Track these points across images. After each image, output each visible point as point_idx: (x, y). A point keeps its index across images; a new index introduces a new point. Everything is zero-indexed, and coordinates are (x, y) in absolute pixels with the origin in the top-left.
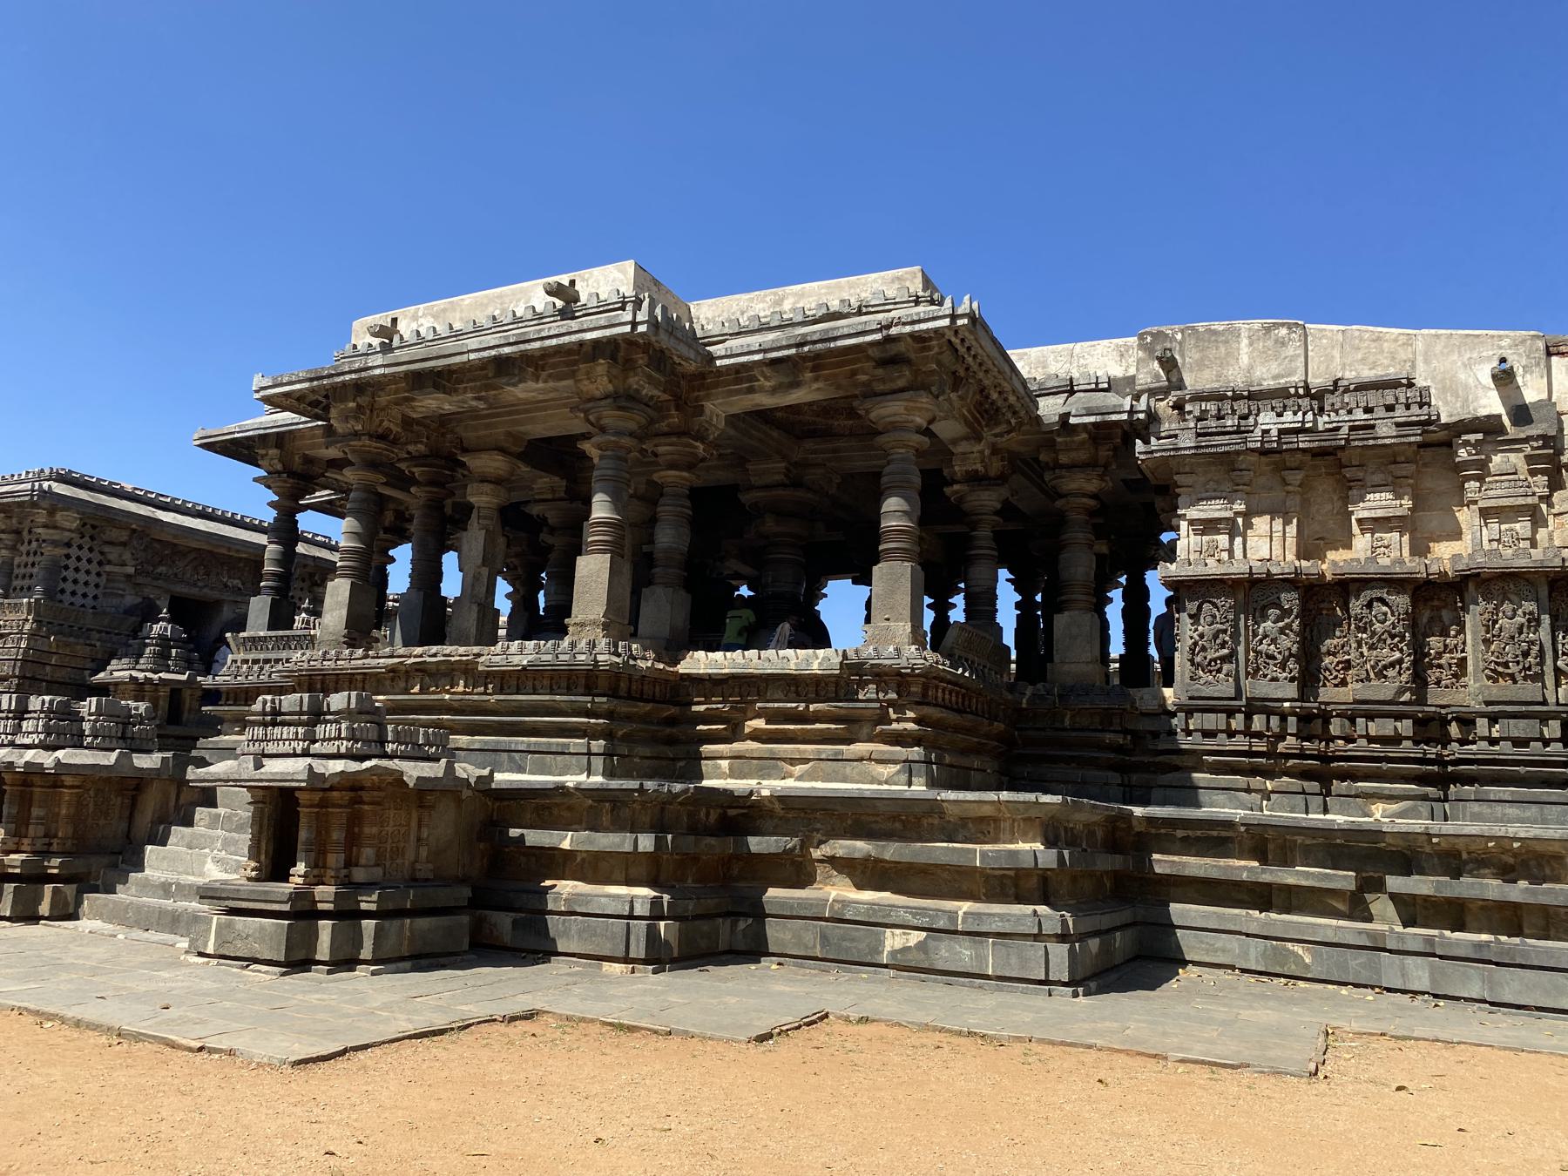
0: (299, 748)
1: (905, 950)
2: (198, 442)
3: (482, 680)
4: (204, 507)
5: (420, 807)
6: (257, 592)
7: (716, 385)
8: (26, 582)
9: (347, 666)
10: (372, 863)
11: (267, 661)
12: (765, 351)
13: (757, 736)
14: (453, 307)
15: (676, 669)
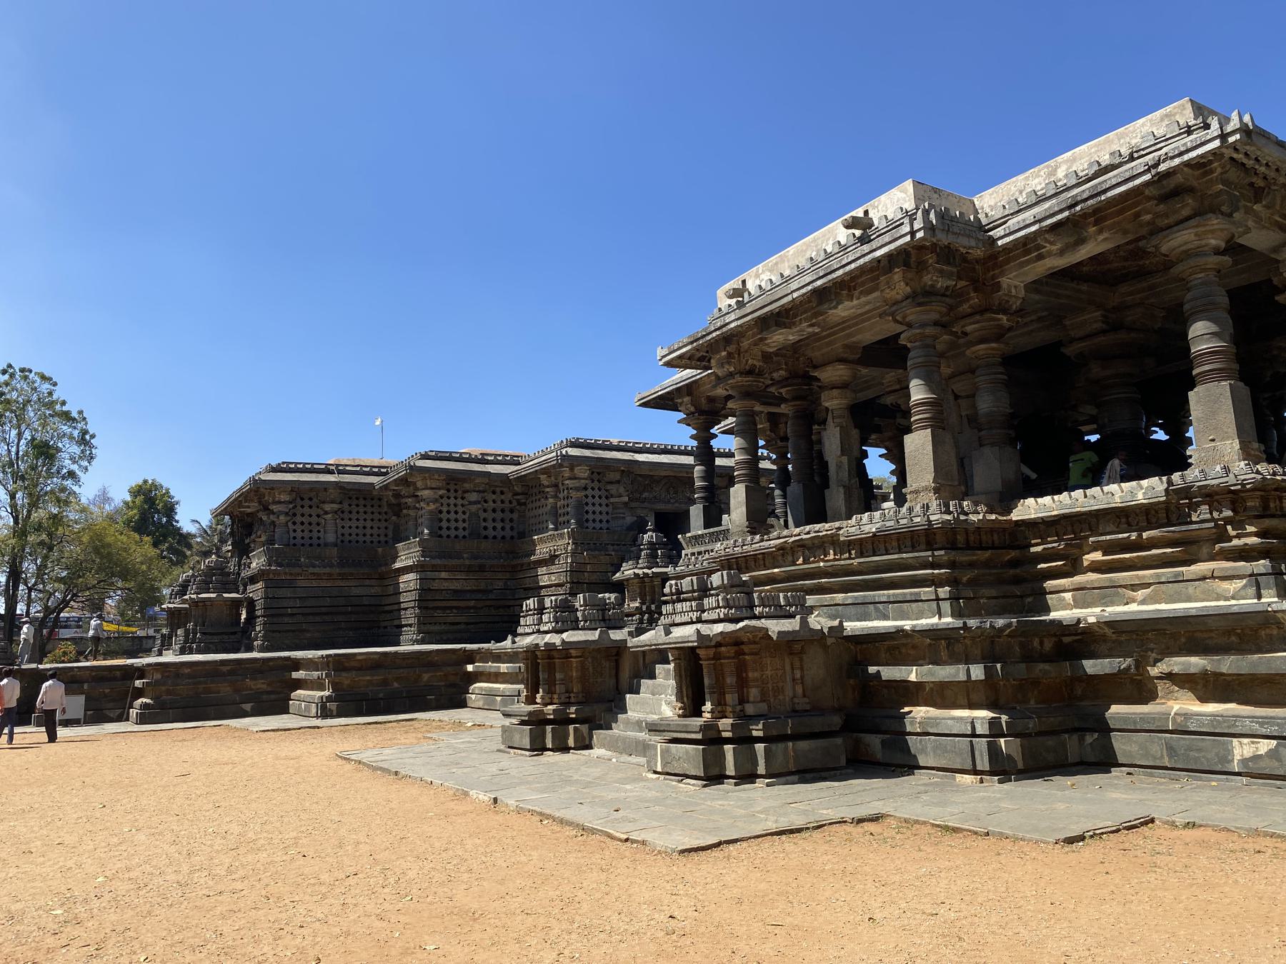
0: (694, 616)
1: (1256, 758)
2: (638, 404)
3: (846, 549)
4: (666, 446)
5: (791, 654)
6: (693, 502)
7: (1008, 261)
8: (566, 518)
9: (749, 549)
10: (759, 699)
11: (699, 553)
12: (1040, 221)
13: (1097, 568)
14: (782, 260)
15: (1009, 518)
